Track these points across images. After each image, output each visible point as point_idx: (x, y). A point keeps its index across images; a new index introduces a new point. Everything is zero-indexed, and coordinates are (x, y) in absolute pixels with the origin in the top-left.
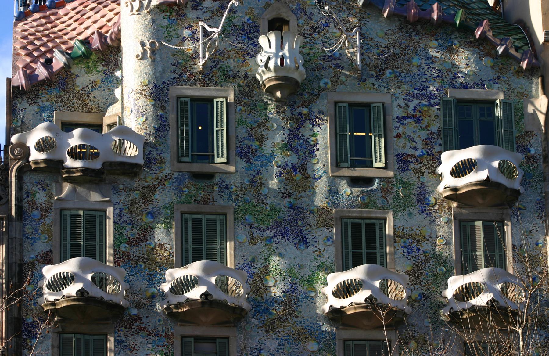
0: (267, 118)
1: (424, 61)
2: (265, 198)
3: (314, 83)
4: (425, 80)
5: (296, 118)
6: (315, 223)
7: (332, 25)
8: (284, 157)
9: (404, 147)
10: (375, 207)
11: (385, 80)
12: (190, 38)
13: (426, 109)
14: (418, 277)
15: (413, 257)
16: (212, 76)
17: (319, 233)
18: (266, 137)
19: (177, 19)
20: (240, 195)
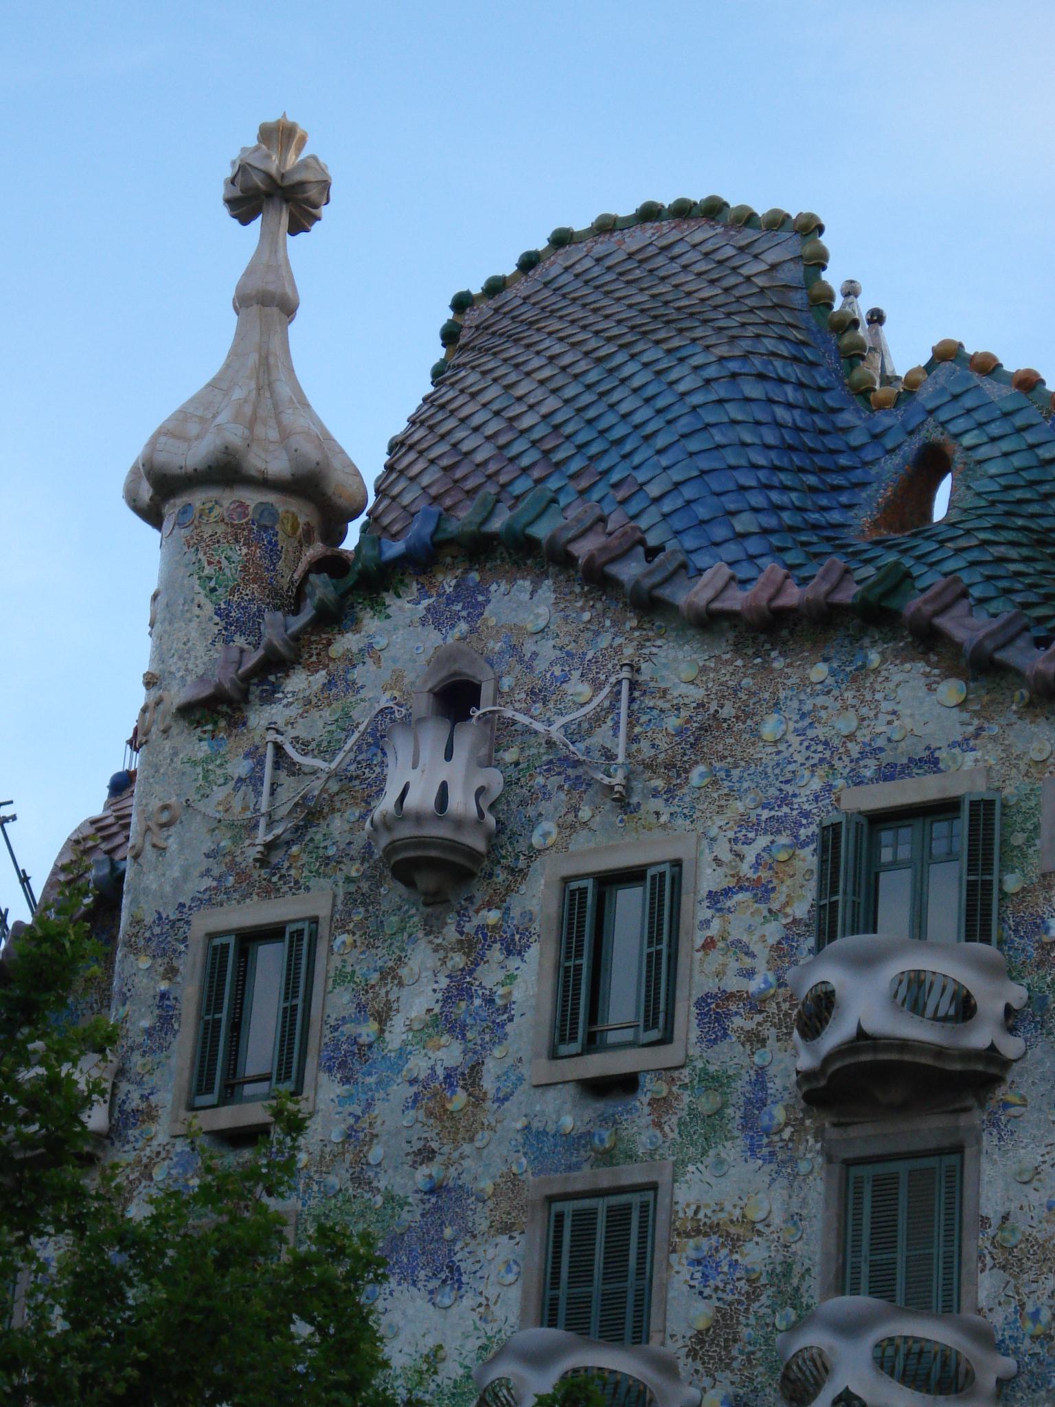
0: (403, 955)
1: (792, 725)
2: (377, 1173)
3: (521, 839)
4: (789, 776)
5: (469, 941)
6: (484, 1226)
7: (576, 674)
8: (430, 1054)
9: (719, 974)
10: (631, 1157)
11: (687, 799)
12: (250, 778)
13: (783, 856)
14: (726, 1348)
15: (716, 1289)
16: (289, 868)
17: (491, 1252)
18: (395, 1006)
19: (229, 736)
20: (316, 1177)
